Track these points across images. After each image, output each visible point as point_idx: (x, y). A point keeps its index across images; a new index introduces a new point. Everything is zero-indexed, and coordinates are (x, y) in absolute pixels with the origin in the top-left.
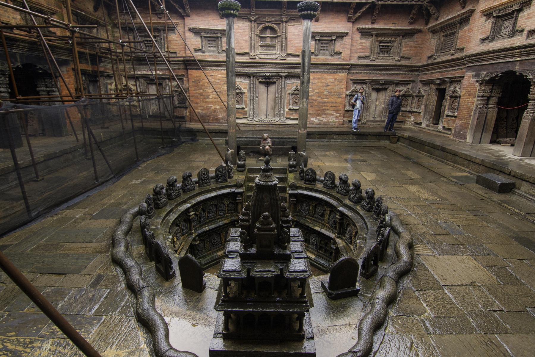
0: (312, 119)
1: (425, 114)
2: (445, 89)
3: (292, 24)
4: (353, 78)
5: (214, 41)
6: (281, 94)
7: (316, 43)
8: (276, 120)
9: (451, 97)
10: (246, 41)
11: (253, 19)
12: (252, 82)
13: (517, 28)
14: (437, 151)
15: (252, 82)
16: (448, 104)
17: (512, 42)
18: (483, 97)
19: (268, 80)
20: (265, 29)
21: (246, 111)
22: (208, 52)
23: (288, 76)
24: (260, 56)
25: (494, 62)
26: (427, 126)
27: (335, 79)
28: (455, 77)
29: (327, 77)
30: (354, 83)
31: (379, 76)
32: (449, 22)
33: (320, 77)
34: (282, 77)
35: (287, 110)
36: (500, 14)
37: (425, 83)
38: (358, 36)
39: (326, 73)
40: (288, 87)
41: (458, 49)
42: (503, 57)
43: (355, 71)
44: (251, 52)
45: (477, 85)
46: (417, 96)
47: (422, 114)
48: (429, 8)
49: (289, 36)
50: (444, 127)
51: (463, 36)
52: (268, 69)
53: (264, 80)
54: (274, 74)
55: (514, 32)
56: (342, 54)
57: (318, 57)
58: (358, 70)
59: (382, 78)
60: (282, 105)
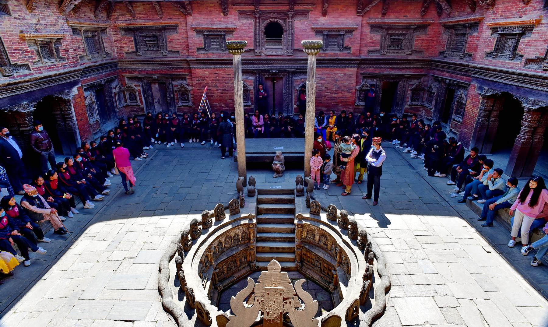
1: (435, 111)
2: (454, 91)
4: (362, 72)
6: (289, 90)
9: (458, 102)
10: (250, 38)
11: (257, 16)
12: (257, 79)
13: (517, 52)
16: (455, 108)
17: (511, 65)
18: (485, 110)
22: (212, 50)
24: (266, 53)
25: (495, 80)
27: (345, 74)
29: (336, 72)
30: (364, 78)
36: (505, 32)
38: (367, 30)
39: (335, 68)
40: (295, 83)
41: (467, 54)
43: (365, 66)
44: (256, 49)
45: (480, 98)
48: (441, 4)
49: (296, 31)
50: (451, 130)
51: (471, 41)
54: (281, 71)
55: (514, 55)
57: (327, 52)
59: (392, 72)
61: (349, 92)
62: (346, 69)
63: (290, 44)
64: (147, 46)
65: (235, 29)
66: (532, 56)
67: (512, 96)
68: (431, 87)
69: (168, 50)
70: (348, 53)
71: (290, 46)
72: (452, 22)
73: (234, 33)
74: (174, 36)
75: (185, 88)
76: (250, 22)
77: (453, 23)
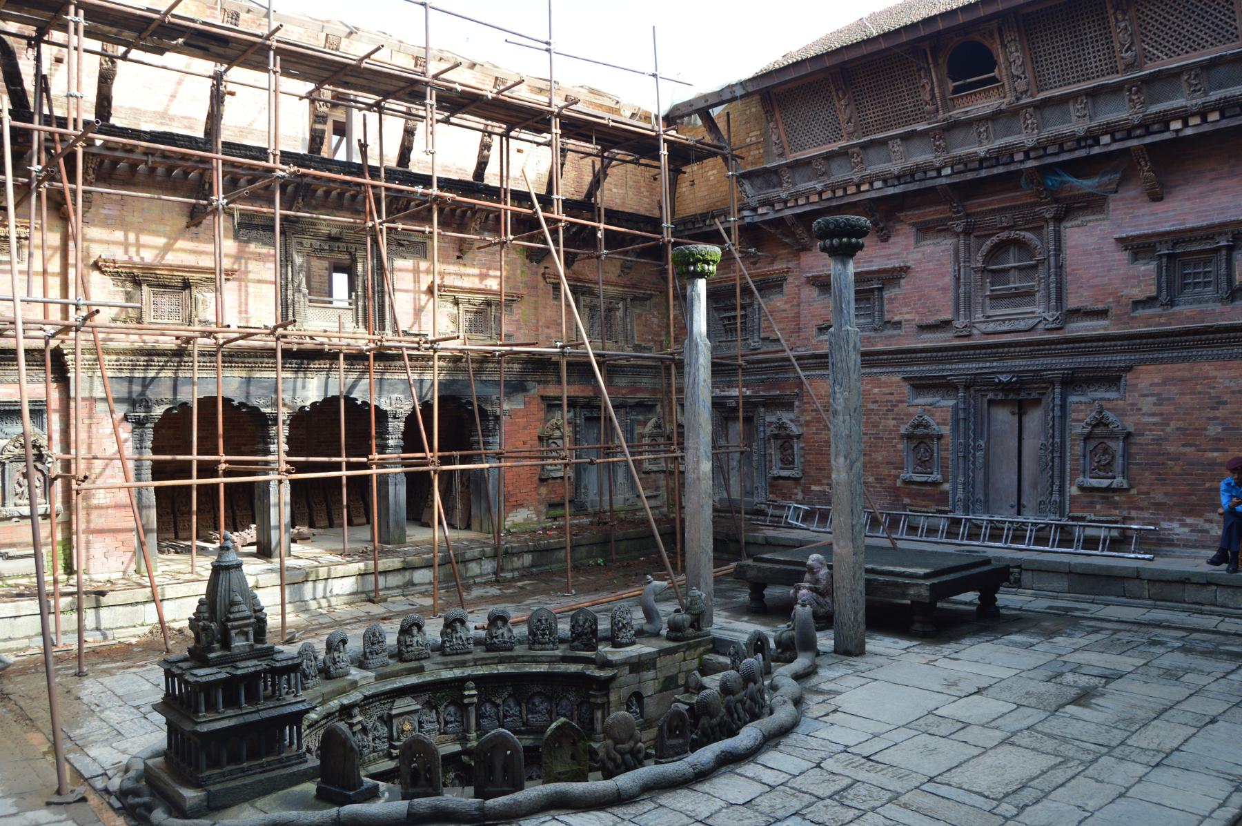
0: (1165, 525)
3: (1079, 222)
5: (868, 299)
7: (1159, 267)
10: (944, 289)
19: (1011, 396)
20: (1000, 249)
21: (947, 493)
23: (1072, 381)
24: (982, 327)
29: (1213, 373)
33: (1185, 374)
34: (1053, 383)
35: (1074, 490)
39: (1210, 359)
40: (1074, 416)
49: (1071, 257)
52: (1009, 363)
53: (1000, 396)
63: (1053, 296)
64: (726, 331)
65: (901, 269)
69: (762, 335)
71: (1053, 303)
73: (902, 281)
74: (778, 302)
75: (786, 428)
76: (943, 248)
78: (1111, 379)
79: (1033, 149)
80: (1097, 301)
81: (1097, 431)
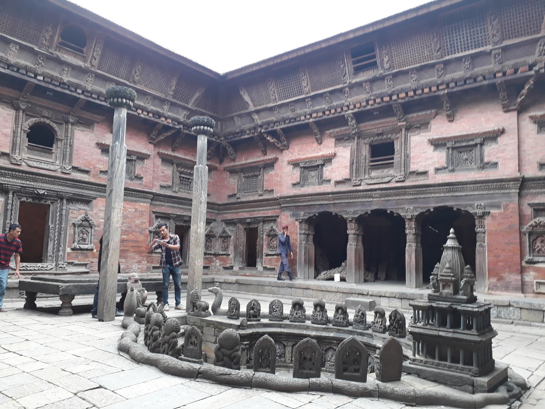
1: (235, 257)
4: (154, 210)
6: (61, 223)
8: (50, 267)
9: (268, 235)
14: (283, 289)
15: (10, 201)
23: (72, 200)
26: (240, 268)
27: (136, 210)
28: (269, 217)
31: (181, 211)
32: (251, 165)
34: (62, 199)
35: (68, 250)
37: (230, 223)
38: (159, 161)
42: (319, 200)
43: (157, 203)
45: (297, 223)
46: (221, 237)
47: (231, 256)
48: (227, 148)
49: (76, 144)
50: (265, 268)
51: (269, 179)
56: (144, 179)
58: (161, 201)
60: (62, 240)
61: (141, 233)
62: (138, 204)
66: (339, 178)
67: (331, 213)
68: (224, 232)
70: (140, 184)
72: (241, 165)
77: (243, 167)
78: (87, 201)
79: (88, 92)
80: (86, 166)
81: (84, 223)
